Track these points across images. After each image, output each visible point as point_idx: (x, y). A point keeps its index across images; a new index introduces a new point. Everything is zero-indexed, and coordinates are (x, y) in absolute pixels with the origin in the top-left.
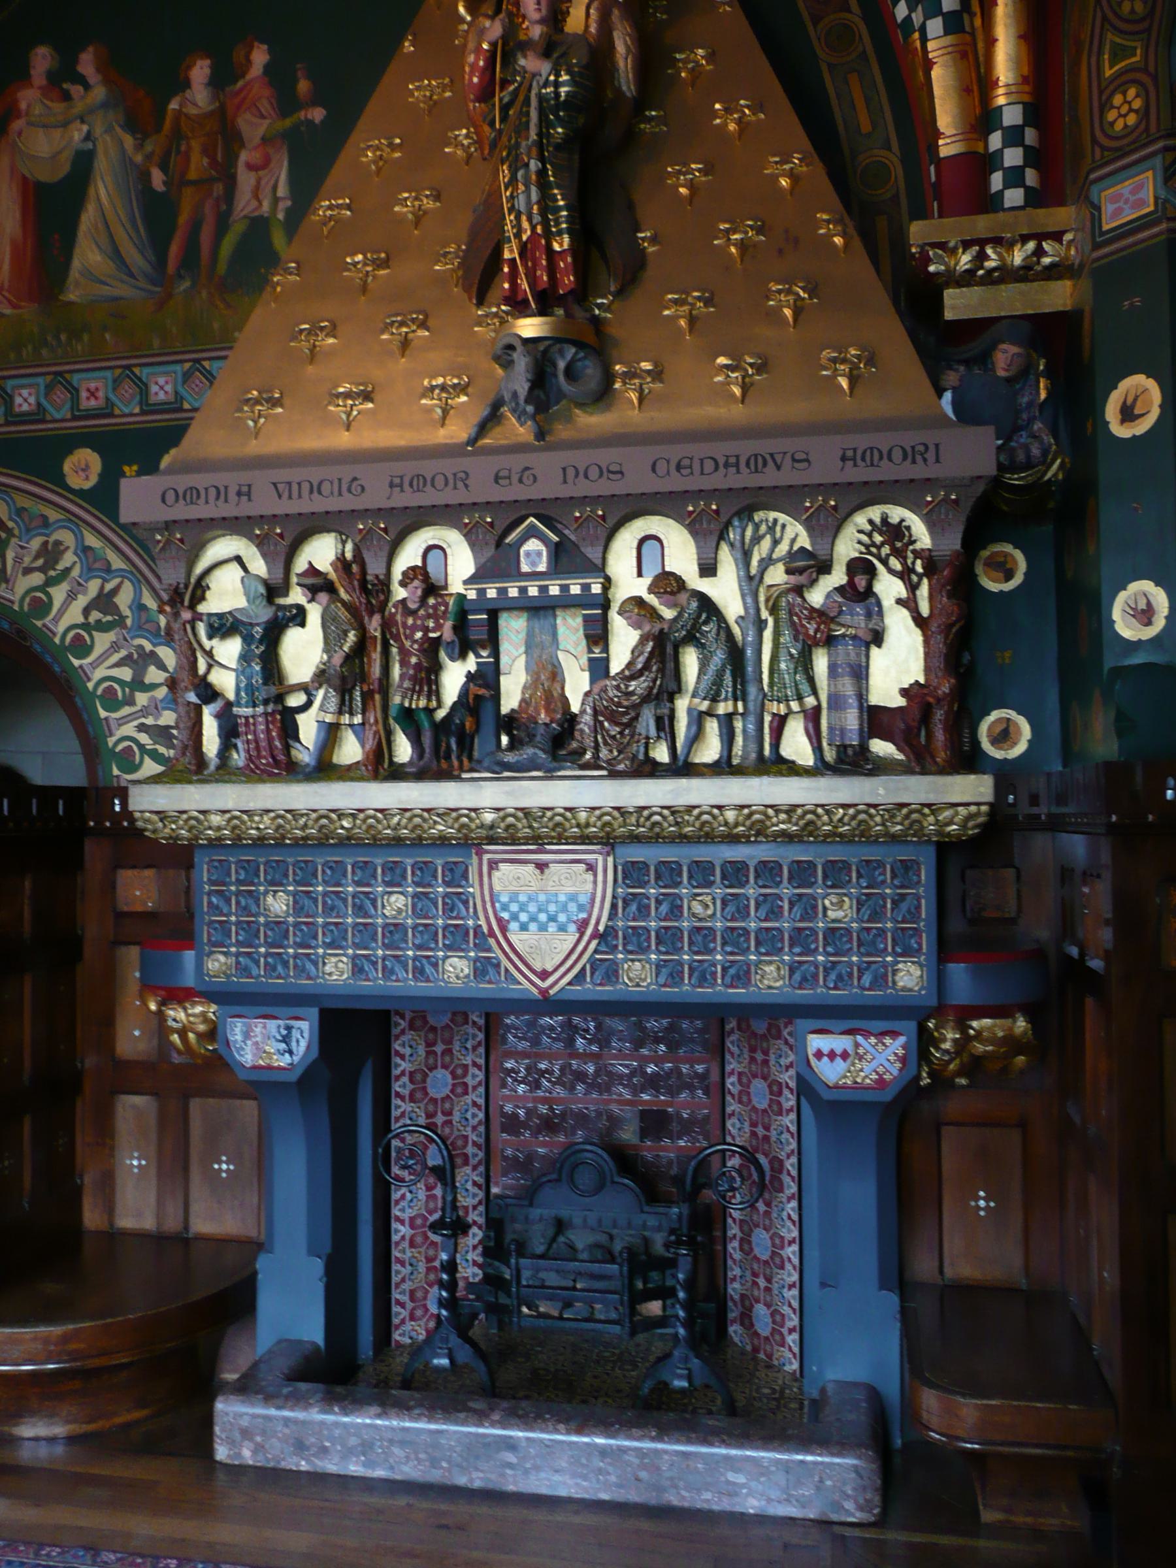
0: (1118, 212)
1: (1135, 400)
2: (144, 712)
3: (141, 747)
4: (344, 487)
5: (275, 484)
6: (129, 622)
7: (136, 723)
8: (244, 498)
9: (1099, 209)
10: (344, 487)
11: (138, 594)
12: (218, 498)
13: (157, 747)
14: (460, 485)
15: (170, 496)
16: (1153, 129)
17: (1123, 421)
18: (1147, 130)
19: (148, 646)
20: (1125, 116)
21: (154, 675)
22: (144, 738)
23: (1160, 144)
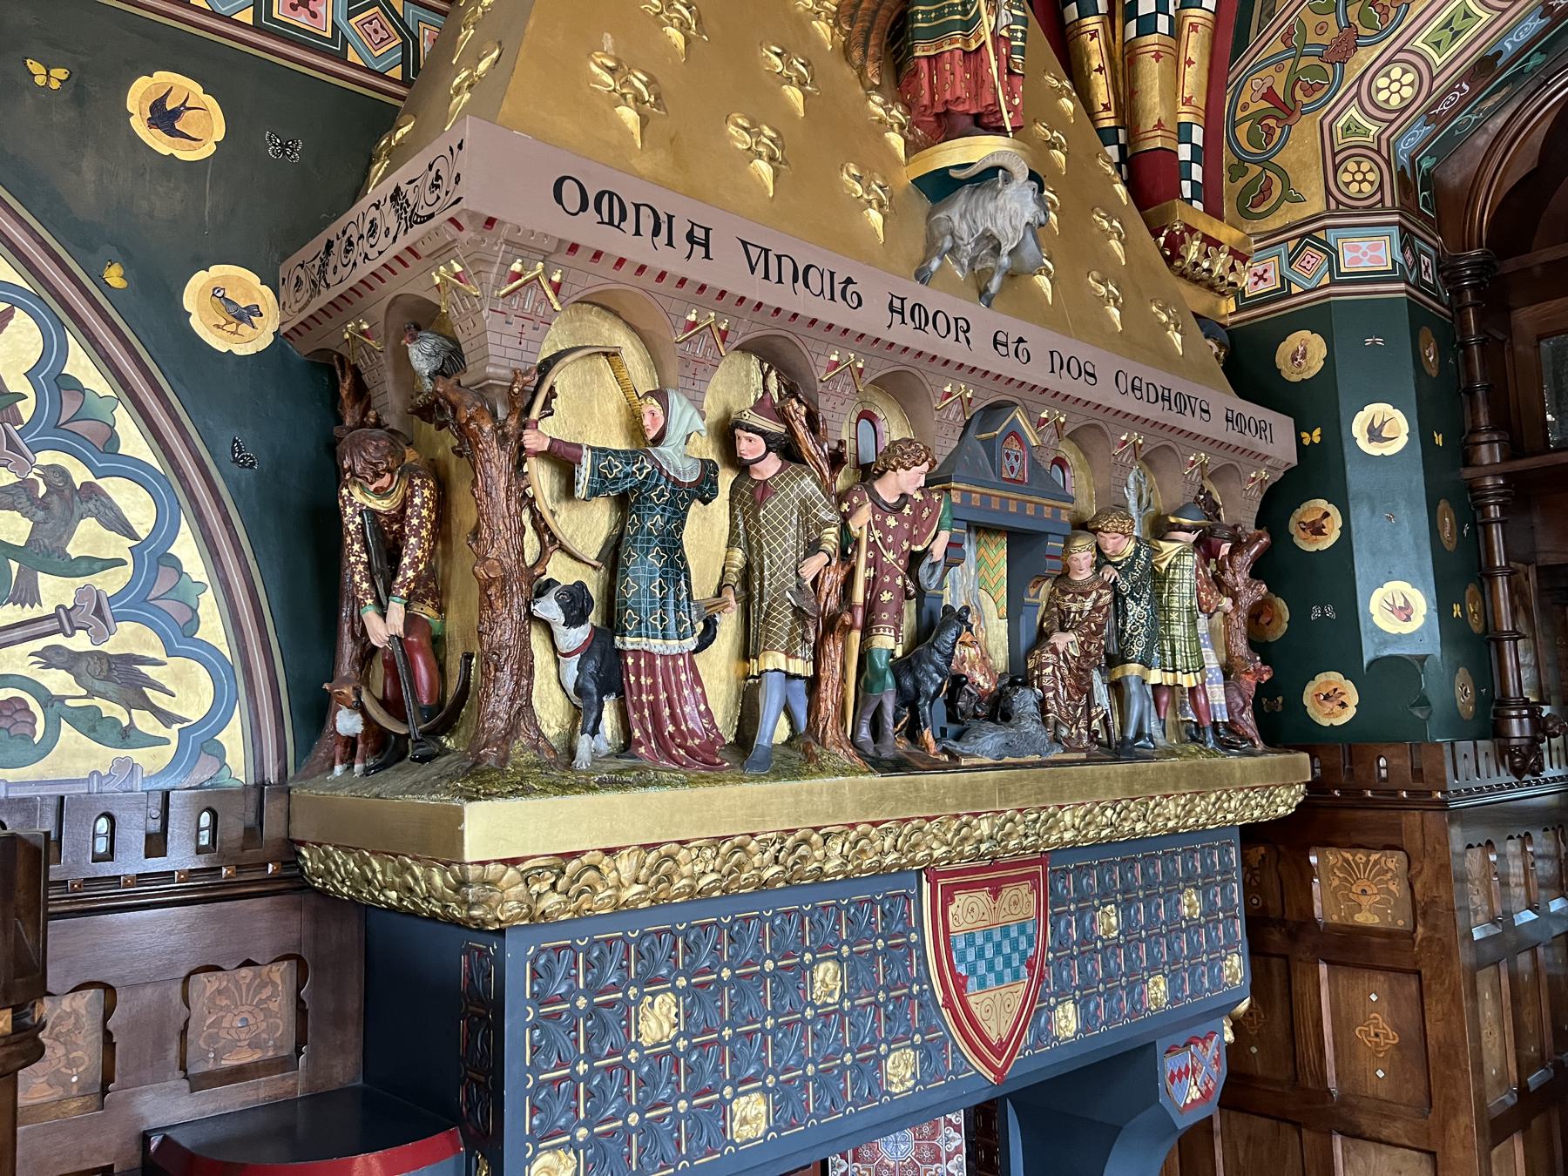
0: (1354, 260)
1: (1383, 424)
2: (64, 620)
3: (49, 701)
4: (838, 288)
5: (744, 244)
6: (26, 409)
7: (39, 645)
8: (699, 251)
9: (1337, 253)
10: (838, 288)
11: (53, 352)
12: (656, 232)
13: (97, 701)
14: (961, 335)
15: (570, 192)
16: (1388, 203)
17: (1370, 440)
18: (1382, 200)
19: (80, 474)
20: (1360, 182)
21: (87, 537)
22: (58, 681)
23: (1396, 218)
